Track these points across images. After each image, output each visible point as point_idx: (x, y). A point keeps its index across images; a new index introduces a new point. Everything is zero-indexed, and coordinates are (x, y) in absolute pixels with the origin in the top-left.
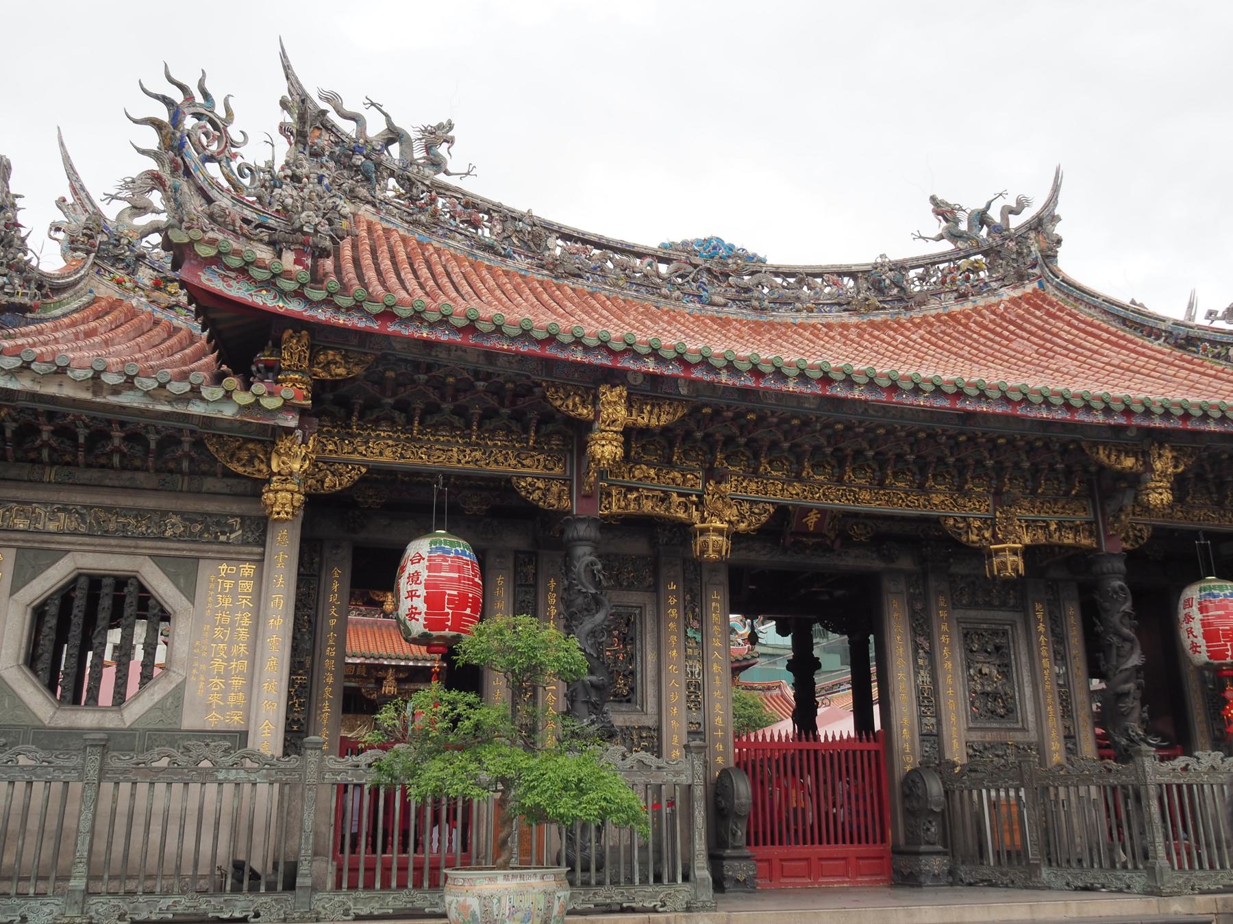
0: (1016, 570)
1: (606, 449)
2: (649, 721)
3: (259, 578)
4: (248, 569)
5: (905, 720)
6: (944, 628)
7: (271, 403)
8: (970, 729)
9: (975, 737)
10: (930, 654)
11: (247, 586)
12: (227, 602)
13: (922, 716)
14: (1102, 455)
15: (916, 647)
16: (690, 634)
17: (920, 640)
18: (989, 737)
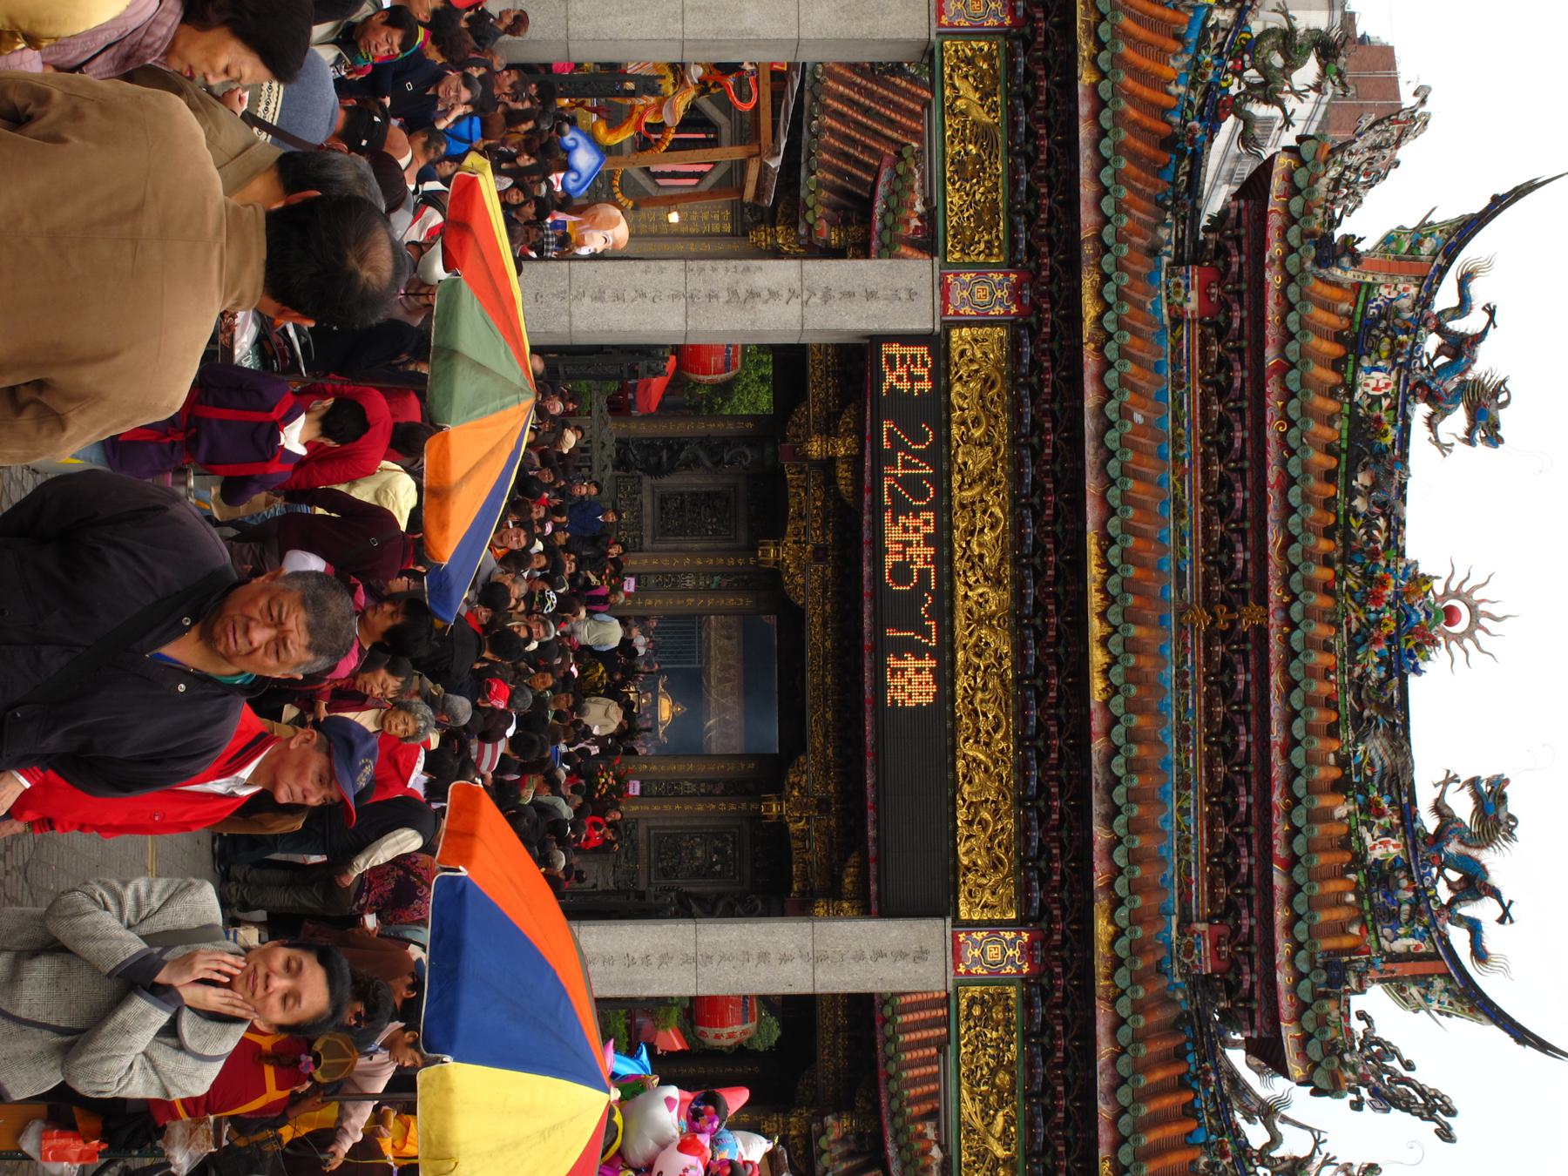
0: (765, 817)
1: (815, 448)
2: (647, 543)
3: (722, 235)
4: (728, 228)
5: (654, 768)
6: (732, 807)
7: (810, 218)
8: (649, 829)
9: (642, 832)
10: (709, 794)
11: (716, 228)
12: (705, 217)
13: (659, 783)
14: (852, 861)
15: (714, 782)
16: (716, 578)
17: (721, 786)
18: (643, 847)
